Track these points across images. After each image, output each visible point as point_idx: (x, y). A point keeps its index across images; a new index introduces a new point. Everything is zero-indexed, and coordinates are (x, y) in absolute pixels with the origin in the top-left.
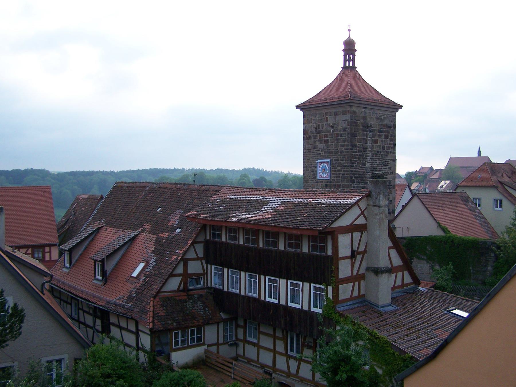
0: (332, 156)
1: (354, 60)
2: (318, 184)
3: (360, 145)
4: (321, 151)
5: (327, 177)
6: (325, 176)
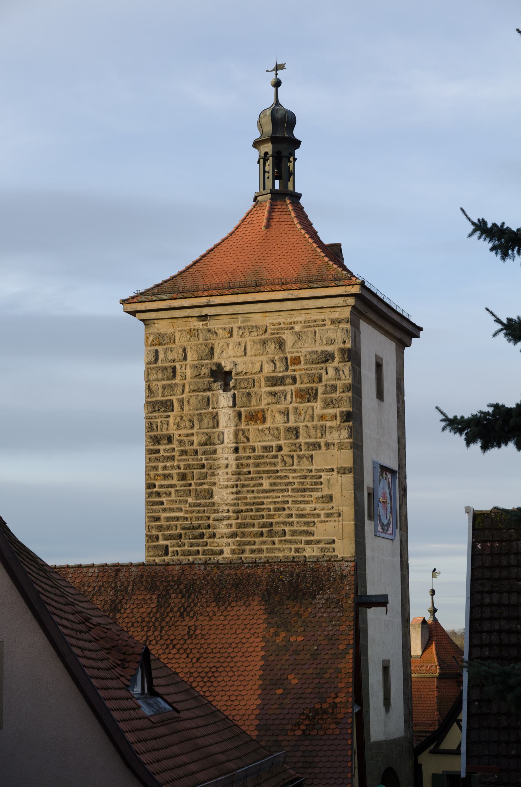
3: (187, 435)
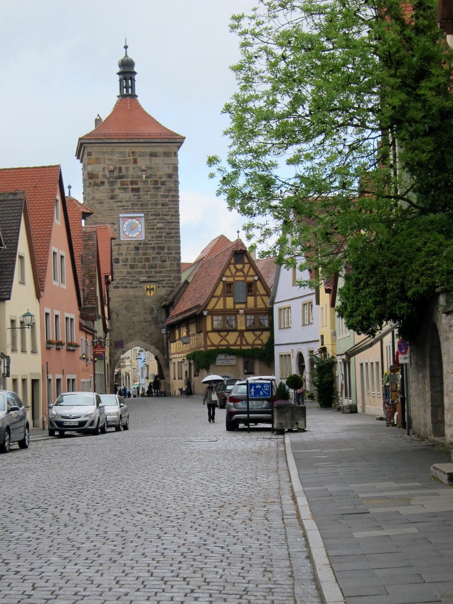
0: (147, 209)
1: (133, 87)
2: (121, 247)
4: (124, 202)
5: (140, 236)
6: (135, 235)
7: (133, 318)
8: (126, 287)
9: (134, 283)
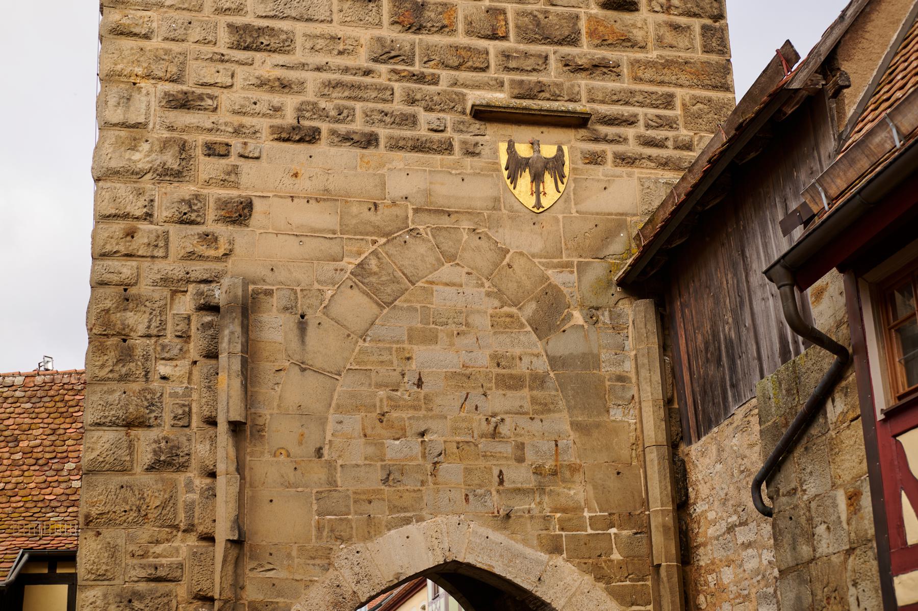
7: (421, 354)
8: (370, 141)
9: (424, 117)
